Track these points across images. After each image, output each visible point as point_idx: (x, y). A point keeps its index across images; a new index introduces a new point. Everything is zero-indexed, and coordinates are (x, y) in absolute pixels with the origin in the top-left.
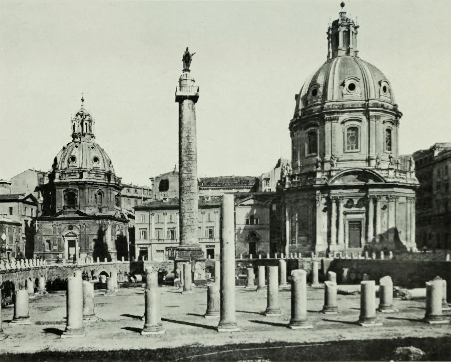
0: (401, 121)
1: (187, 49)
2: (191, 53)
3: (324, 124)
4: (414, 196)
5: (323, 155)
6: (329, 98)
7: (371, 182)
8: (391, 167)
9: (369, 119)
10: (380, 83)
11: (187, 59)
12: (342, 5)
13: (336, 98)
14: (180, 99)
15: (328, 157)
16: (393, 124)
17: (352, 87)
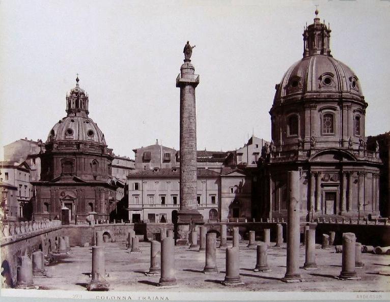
0: (367, 110)
1: (188, 43)
2: (191, 45)
3: (304, 110)
4: (378, 172)
5: (303, 136)
6: (309, 89)
7: (345, 160)
8: (361, 148)
9: (342, 108)
10: (350, 79)
11: (188, 50)
12: (317, 13)
13: (314, 89)
14: (181, 85)
15: (307, 138)
16: (361, 112)
17: (328, 81)
